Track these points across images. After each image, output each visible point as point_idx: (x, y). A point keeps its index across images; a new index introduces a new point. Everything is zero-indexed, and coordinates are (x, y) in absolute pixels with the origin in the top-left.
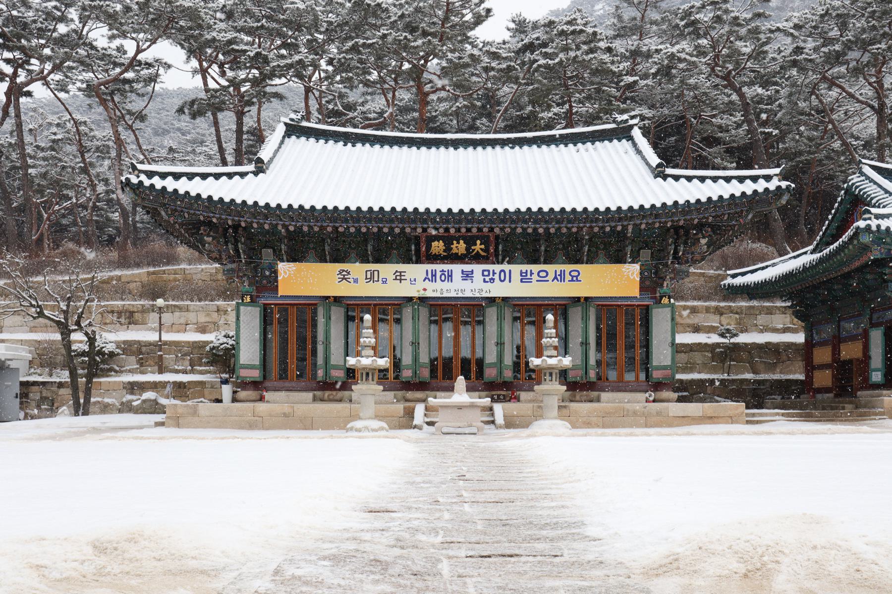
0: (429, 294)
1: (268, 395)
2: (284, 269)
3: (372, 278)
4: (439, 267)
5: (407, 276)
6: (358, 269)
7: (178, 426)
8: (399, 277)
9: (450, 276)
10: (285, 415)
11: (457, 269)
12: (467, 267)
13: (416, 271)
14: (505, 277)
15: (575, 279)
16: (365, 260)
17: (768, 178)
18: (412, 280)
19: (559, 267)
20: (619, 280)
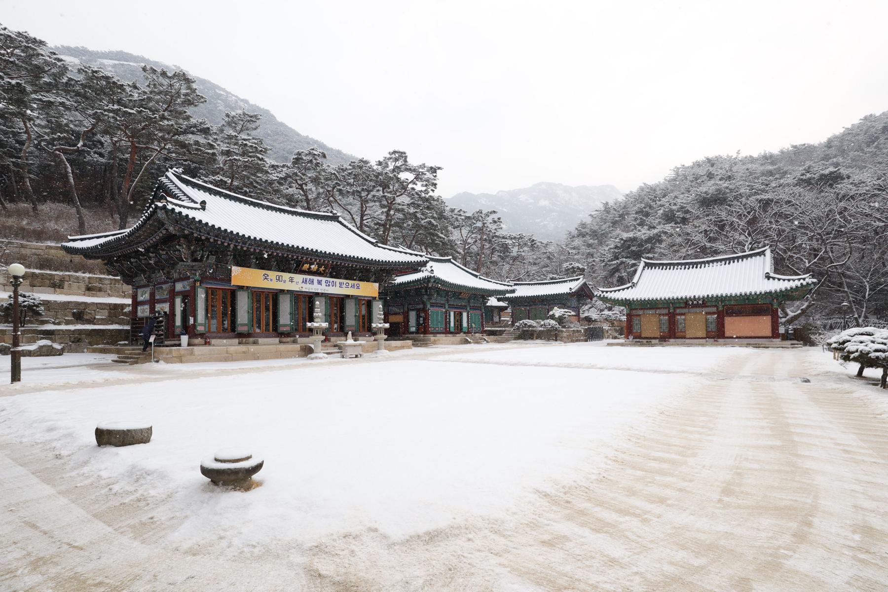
0: (304, 290)
1: (213, 341)
2: (236, 270)
3: (278, 280)
4: (308, 277)
5: (294, 280)
6: (273, 274)
7: (181, 362)
8: (291, 280)
9: (312, 282)
10: (244, 352)
11: (316, 278)
12: (320, 278)
13: (298, 278)
14: (334, 284)
15: (358, 288)
16: (290, 272)
17: (421, 256)
18: (296, 283)
19: (353, 282)
20: (369, 289)
